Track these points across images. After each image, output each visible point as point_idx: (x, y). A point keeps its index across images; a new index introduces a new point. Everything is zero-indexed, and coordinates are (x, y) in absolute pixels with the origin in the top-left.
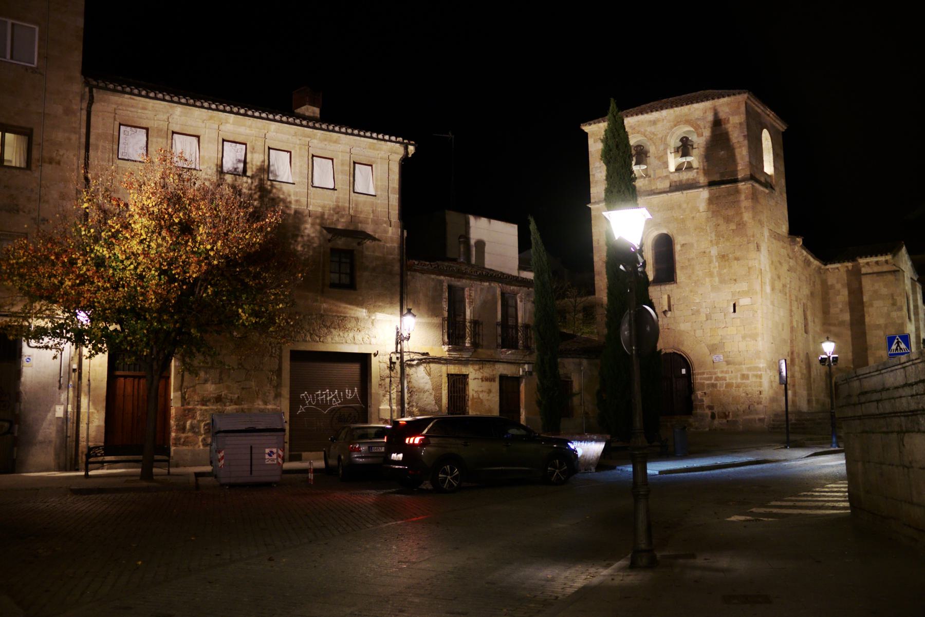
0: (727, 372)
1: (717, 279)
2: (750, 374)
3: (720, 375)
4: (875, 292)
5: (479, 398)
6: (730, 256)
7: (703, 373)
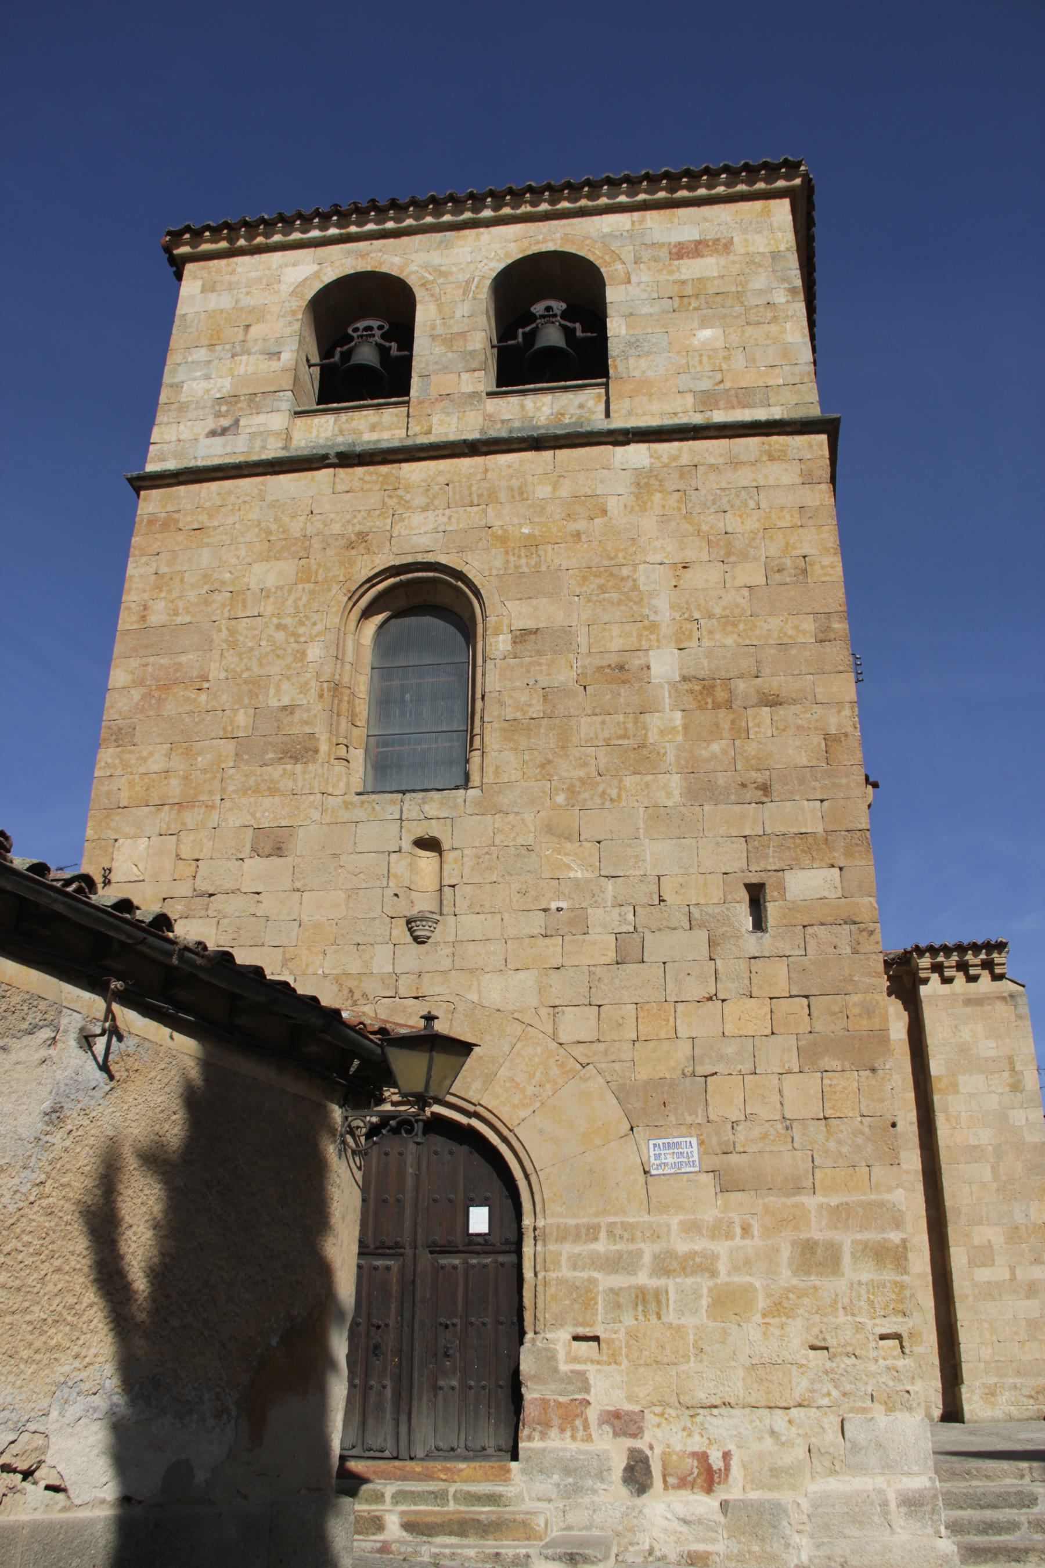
0: (719, 1230)
1: (675, 782)
2: (847, 1240)
3: (682, 1247)
4: (963, 1049)
6: (741, 686)
7: (592, 1232)
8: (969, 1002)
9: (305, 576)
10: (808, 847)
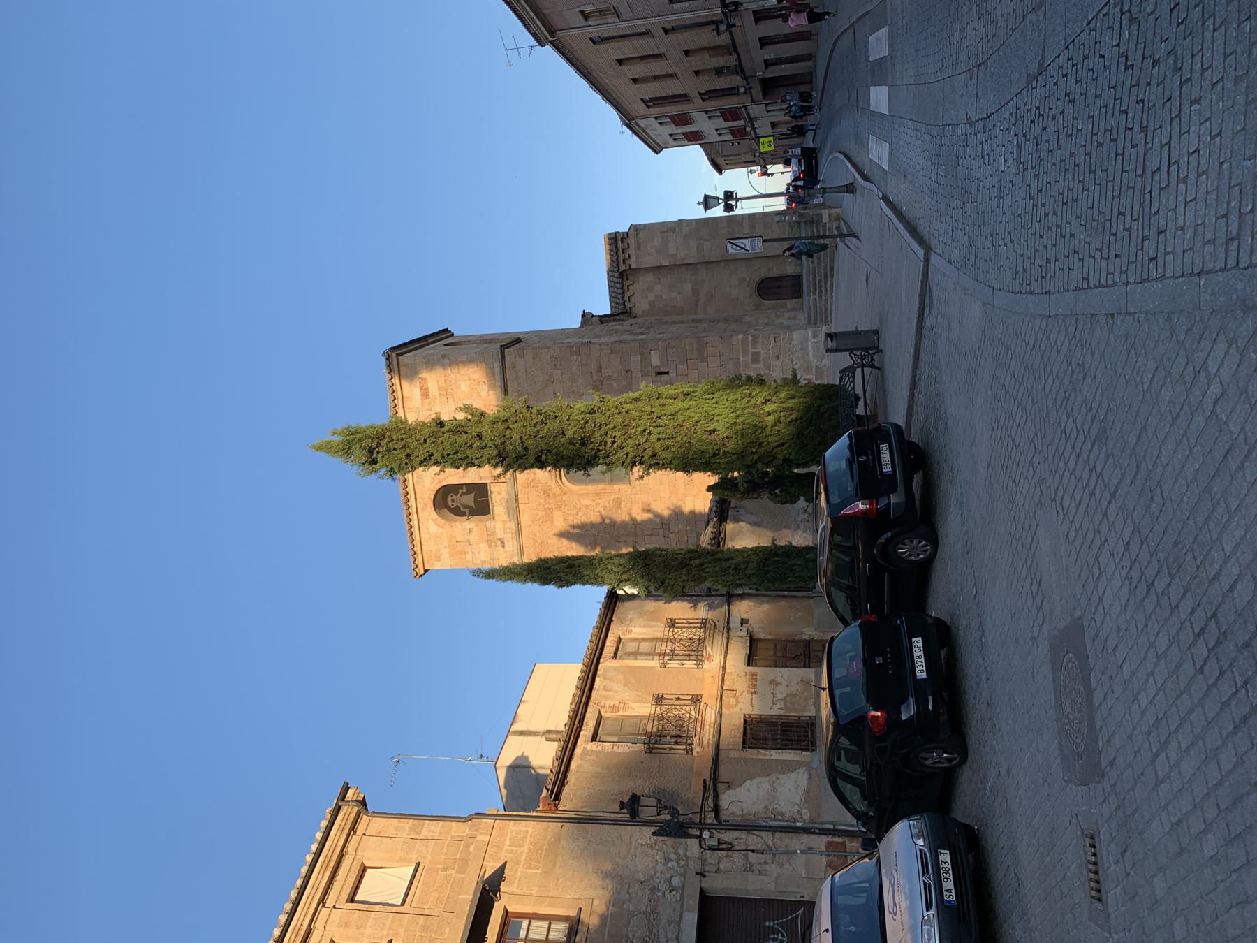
2: (751, 350)
5: (784, 699)
8: (639, 249)
9: (559, 508)
10: (645, 359)
